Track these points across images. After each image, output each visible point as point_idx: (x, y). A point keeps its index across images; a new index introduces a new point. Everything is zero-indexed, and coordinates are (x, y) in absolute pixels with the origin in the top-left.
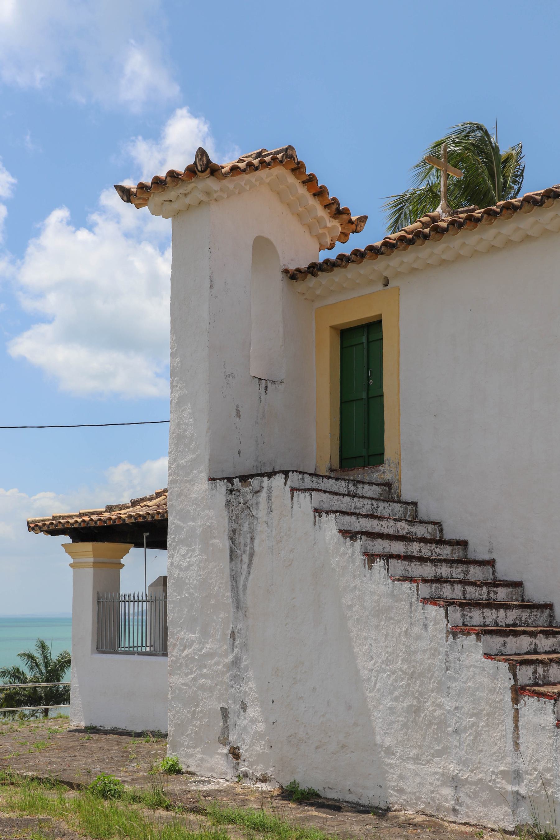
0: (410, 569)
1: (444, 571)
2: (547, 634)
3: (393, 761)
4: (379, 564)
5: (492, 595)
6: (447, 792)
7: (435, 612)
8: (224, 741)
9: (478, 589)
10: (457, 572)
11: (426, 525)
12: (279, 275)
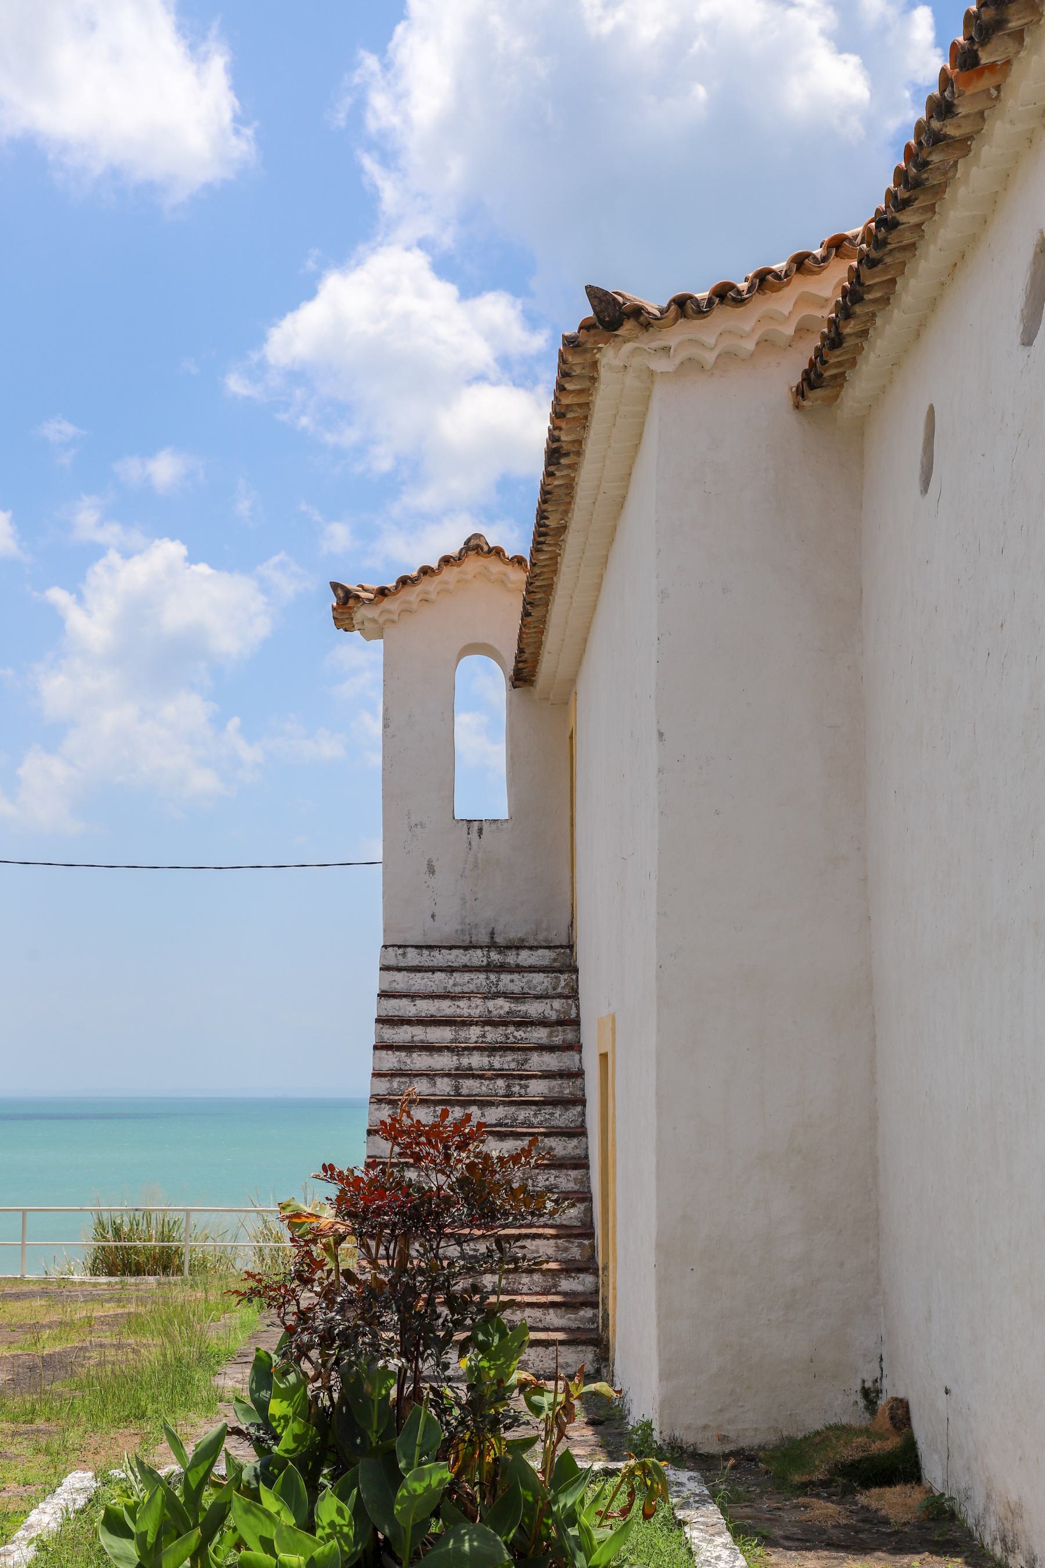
0: (409, 1061)
5: (516, 1089)
9: (487, 1082)
11: (547, 1001)
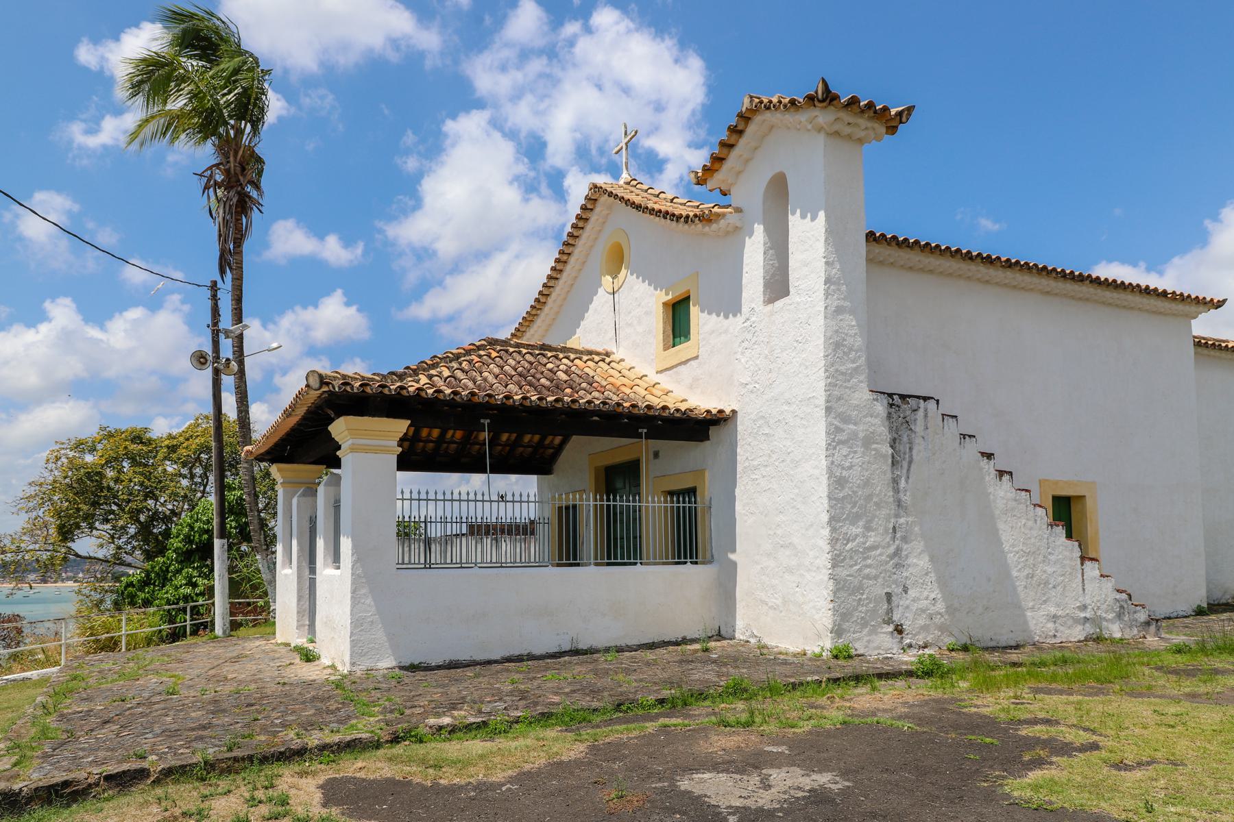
8: (889, 621)
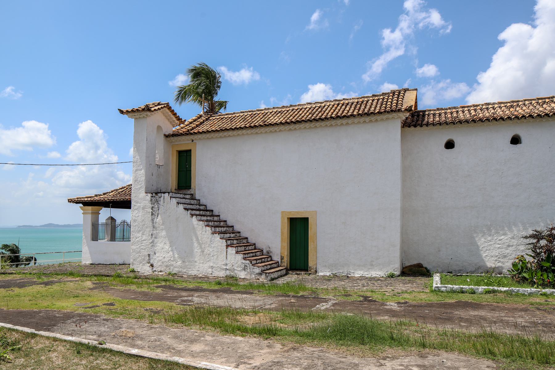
1: (209, 218)
2: (233, 233)
3: (197, 264)
4: (194, 217)
6: (210, 270)
7: (208, 229)
8: (149, 263)
10: (211, 218)
12: (163, 136)
